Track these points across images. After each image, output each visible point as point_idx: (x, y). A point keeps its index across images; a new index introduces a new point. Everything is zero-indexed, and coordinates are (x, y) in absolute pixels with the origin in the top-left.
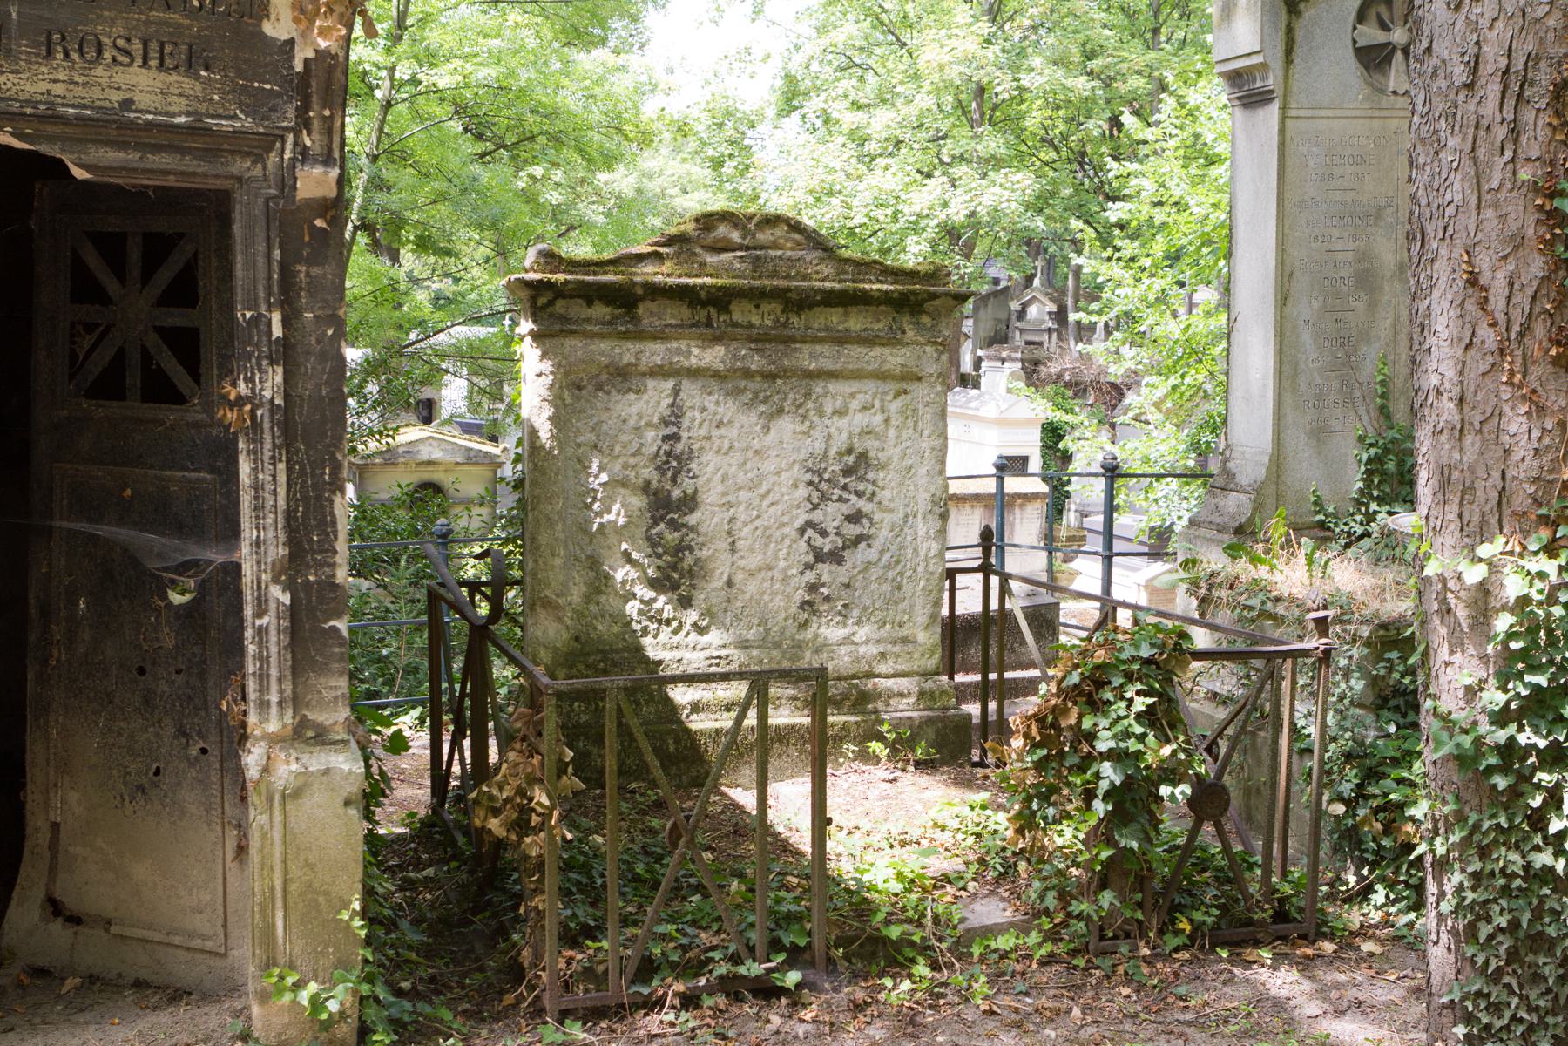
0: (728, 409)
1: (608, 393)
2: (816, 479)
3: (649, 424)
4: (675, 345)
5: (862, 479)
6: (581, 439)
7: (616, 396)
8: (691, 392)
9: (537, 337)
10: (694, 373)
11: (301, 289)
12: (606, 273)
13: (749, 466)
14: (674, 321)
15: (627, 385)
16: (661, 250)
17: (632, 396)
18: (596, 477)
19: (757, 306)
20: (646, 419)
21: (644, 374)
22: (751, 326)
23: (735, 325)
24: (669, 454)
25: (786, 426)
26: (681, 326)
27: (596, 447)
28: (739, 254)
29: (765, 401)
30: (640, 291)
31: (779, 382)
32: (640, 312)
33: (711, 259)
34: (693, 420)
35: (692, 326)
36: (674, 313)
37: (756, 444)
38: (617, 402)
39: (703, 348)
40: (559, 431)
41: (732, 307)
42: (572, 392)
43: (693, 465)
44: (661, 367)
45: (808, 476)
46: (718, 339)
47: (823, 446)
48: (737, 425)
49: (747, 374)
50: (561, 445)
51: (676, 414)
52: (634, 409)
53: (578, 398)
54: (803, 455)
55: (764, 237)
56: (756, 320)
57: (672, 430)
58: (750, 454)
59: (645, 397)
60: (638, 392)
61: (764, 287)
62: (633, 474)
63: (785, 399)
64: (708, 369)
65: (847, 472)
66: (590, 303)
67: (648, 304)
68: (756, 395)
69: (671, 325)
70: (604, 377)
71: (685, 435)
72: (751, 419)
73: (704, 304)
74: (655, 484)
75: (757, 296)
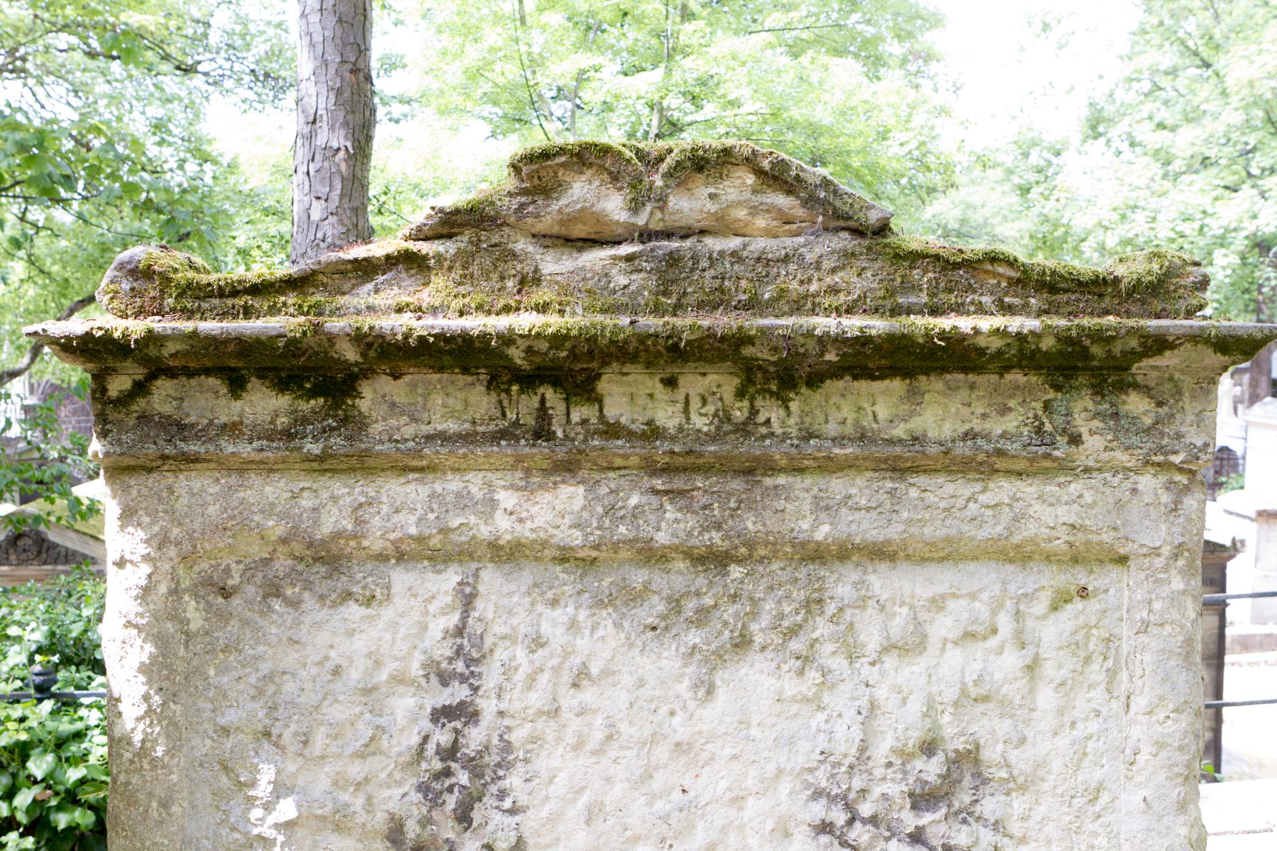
0: (602, 640)
1: (295, 604)
2: (839, 817)
3: (399, 679)
4: (454, 484)
5: (965, 816)
6: (229, 717)
7: (313, 610)
8: (504, 600)
9: (118, 471)
10: (507, 554)
11: (317, 328)
12: (274, 310)
13: (657, 785)
14: (452, 426)
15: (342, 583)
16: (424, 248)
17: (354, 611)
18: (268, 807)
19: (671, 382)
20: (390, 667)
21: (382, 558)
22: (653, 432)
23: (612, 430)
24: (449, 753)
25: (757, 681)
26: (467, 438)
27: (267, 734)
28: (625, 249)
29: (702, 617)
30: (351, 354)
31: (736, 571)
32: (364, 405)
33: (554, 265)
34: (508, 670)
35: (502, 434)
36: (456, 404)
37: (679, 728)
38: (318, 625)
39: (526, 489)
40: (172, 697)
41: (603, 386)
42: (210, 597)
43: (514, 781)
44: (420, 539)
45: (818, 810)
46: (567, 468)
47: (856, 733)
48: (627, 680)
49: (650, 555)
50: (174, 731)
51: (464, 658)
52: (361, 644)
53: (224, 617)
54: (804, 754)
55: (690, 204)
56: (667, 416)
57: (458, 693)
58: (661, 752)
59: (387, 613)
60: (370, 600)
61: (674, 334)
62: (358, 803)
63: (754, 615)
64: (544, 544)
65: (923, 799)
66: (237, 386)
67: (384, 384)
68: (675, 603)
69: (444, 437)
70: (282, 564)
71: (488, 706)
72: (665, 664)
73: (528, 380)
74: (412, 830)
75: (669, 357)
